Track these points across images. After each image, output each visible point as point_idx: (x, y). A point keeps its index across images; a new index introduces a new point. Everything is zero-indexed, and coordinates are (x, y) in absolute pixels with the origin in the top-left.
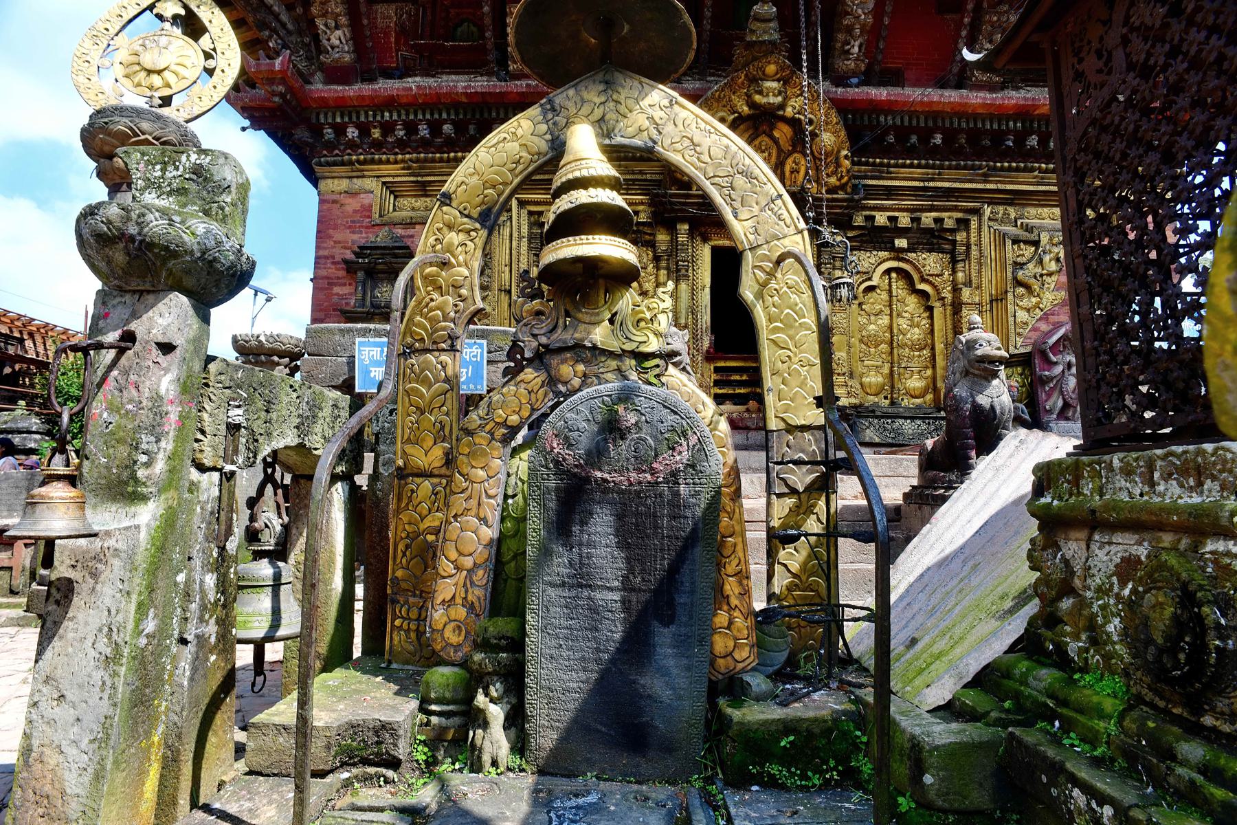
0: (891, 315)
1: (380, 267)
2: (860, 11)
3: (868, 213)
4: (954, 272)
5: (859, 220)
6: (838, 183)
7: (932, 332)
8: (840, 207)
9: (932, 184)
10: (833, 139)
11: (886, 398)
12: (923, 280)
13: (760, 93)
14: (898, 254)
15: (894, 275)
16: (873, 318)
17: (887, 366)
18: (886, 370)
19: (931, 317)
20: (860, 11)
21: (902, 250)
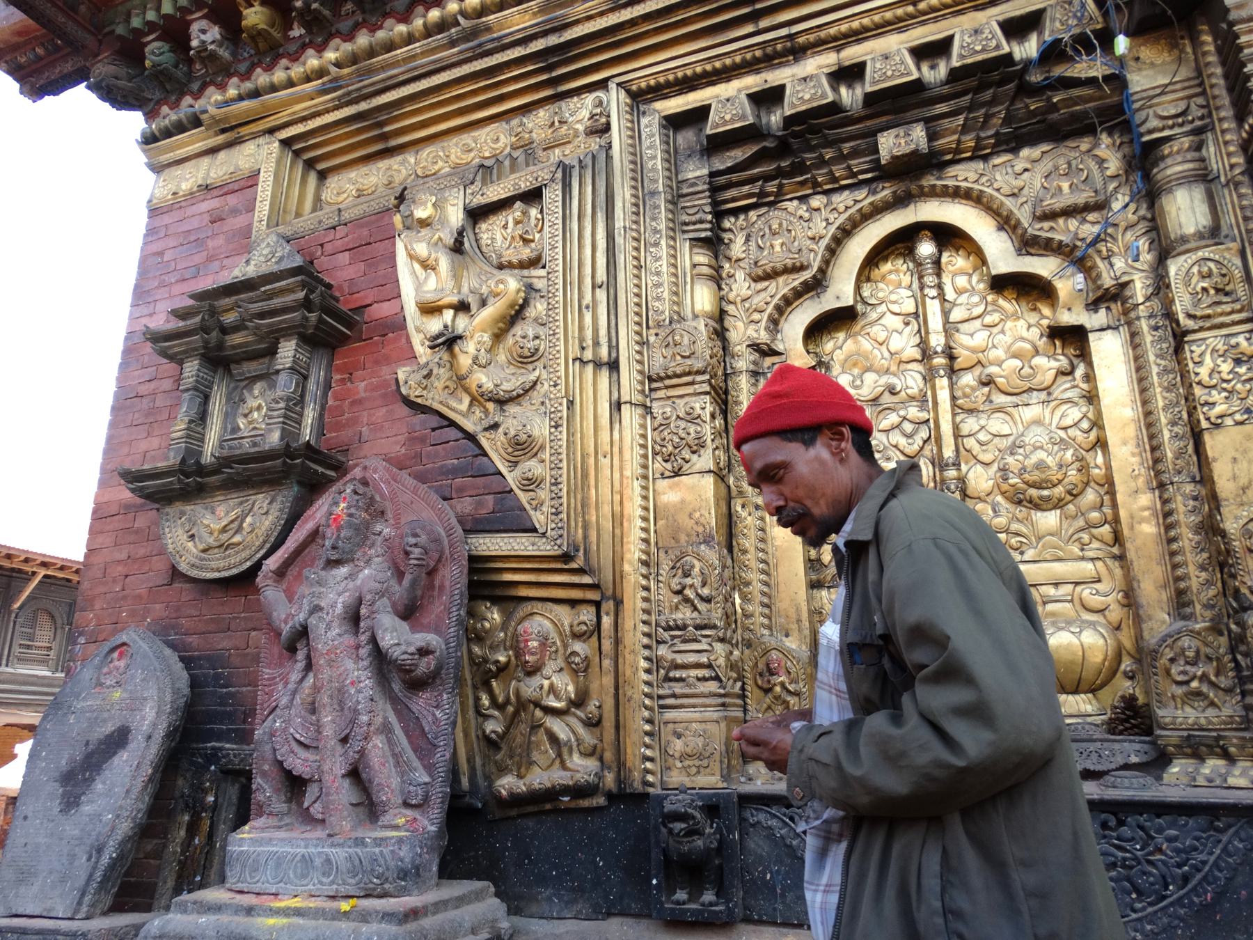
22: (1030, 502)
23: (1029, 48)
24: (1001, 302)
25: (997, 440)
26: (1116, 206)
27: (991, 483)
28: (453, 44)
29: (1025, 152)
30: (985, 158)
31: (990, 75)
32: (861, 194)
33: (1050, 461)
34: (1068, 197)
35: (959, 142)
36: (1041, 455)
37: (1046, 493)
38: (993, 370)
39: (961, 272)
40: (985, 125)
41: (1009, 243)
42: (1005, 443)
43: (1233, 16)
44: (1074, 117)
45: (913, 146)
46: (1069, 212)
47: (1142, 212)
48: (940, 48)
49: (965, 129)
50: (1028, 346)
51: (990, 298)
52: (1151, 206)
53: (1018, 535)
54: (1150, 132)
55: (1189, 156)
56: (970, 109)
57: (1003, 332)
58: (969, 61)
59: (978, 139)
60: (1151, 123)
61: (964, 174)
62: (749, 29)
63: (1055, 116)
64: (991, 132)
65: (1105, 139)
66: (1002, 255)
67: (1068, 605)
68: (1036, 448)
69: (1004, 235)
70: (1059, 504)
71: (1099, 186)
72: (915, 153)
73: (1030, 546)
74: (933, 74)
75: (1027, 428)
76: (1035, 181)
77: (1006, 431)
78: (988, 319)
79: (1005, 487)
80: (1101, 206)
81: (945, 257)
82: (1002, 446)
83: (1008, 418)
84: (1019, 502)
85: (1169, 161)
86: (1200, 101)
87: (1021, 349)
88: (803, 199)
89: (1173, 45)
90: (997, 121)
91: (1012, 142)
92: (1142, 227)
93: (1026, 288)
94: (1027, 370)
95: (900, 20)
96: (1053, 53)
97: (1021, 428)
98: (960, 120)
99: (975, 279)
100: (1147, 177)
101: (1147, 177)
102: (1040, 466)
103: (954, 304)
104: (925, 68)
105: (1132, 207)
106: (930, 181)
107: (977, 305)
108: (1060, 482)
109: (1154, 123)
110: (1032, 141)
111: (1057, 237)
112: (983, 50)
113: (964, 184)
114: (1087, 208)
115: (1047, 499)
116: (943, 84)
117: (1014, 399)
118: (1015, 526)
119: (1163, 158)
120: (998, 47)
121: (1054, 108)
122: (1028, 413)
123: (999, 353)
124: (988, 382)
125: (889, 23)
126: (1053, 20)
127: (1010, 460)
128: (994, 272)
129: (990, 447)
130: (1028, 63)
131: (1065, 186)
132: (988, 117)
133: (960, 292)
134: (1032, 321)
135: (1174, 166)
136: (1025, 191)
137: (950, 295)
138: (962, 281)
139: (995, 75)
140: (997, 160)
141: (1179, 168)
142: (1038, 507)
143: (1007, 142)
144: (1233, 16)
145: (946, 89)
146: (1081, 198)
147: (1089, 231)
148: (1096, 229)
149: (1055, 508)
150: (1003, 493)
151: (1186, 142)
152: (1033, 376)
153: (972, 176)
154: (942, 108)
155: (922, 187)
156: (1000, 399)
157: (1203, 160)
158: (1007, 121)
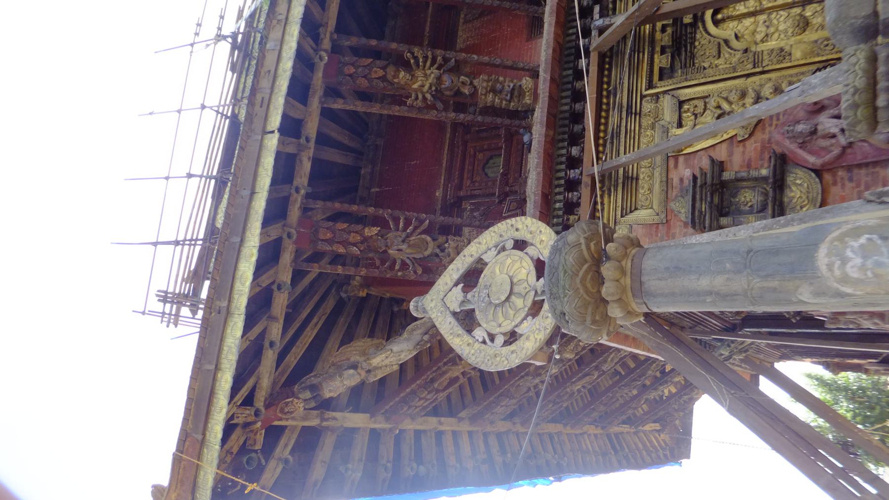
1: (716, 200)
28: (612, 143)
32: (698, 31)
62: (641, 55)
88: (695, 47)
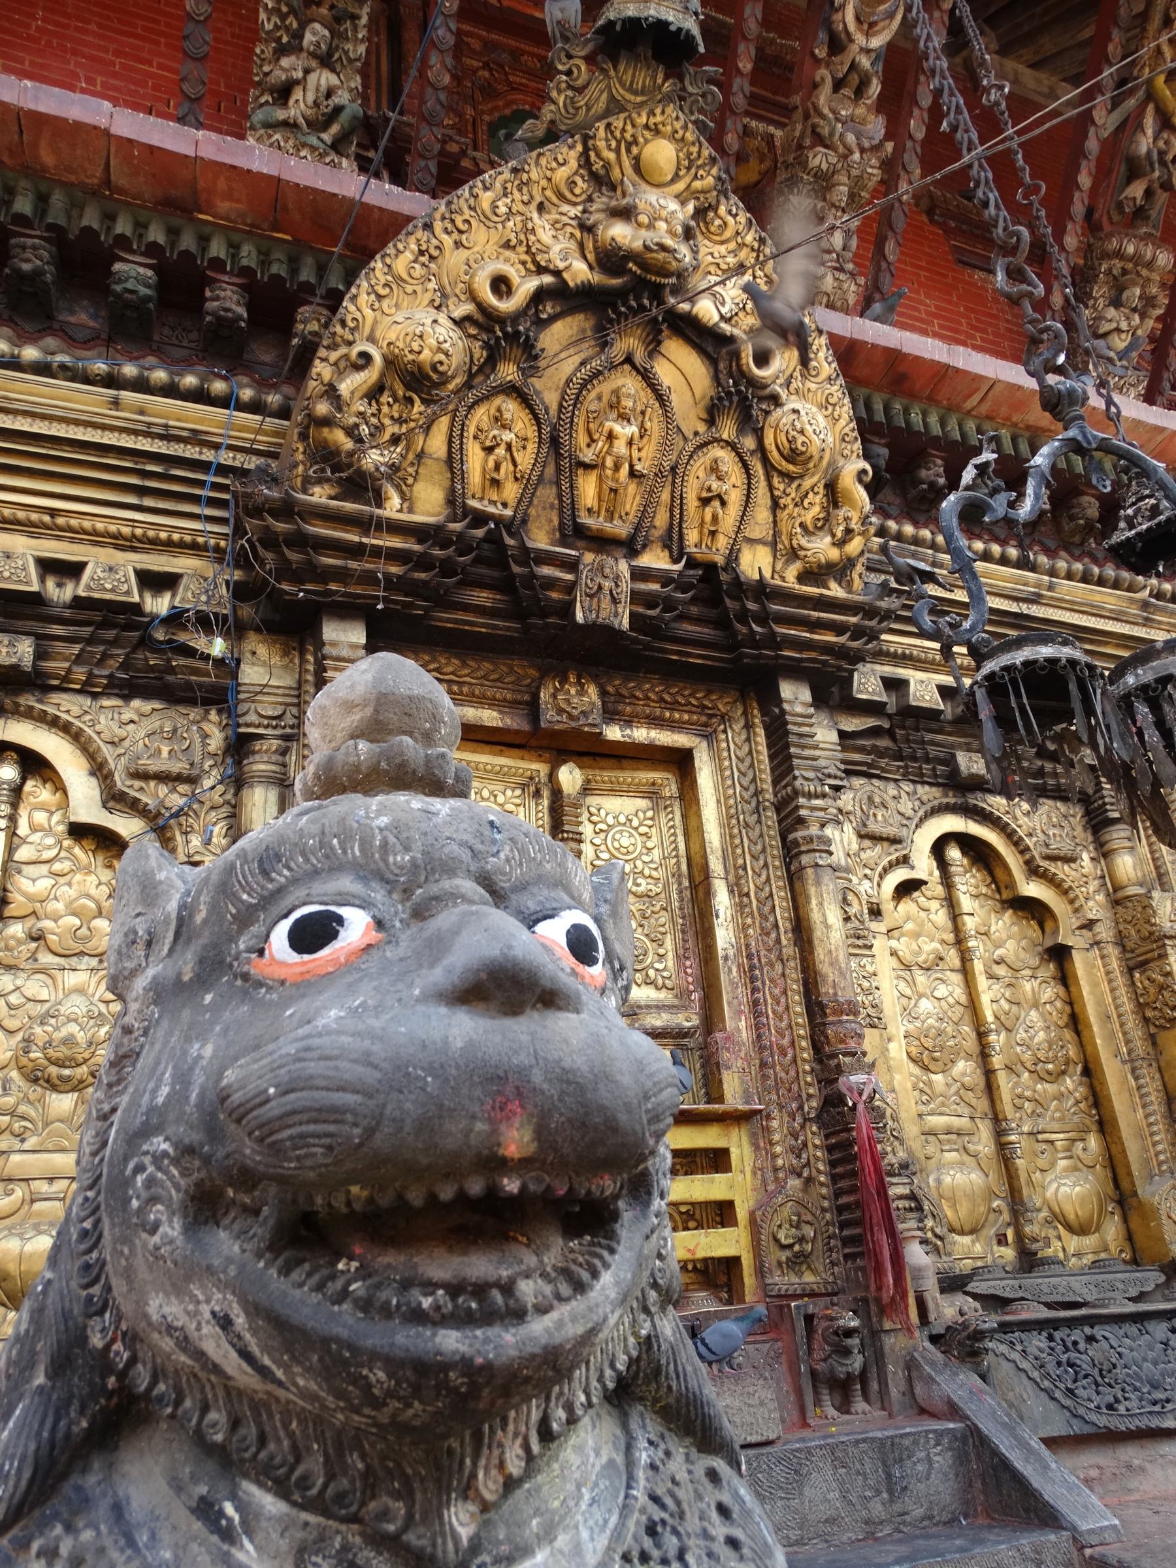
0: (966, 970)
2: (851, 138)
3: (888, 670)
4: (1104, 853)
5: (867, 683)
6: (834, 554)
7: (1075, 1021)
8: (839, 629)
9: (1036, 611)
10: (822, 422)
11: (1002, 1240)
12: (1033, 871)
13: (626, 214)
14: (961, 792)
15: (954, 853)
16: (921, 978)
17: (985, 1131)
18: (984, 1143)
19: (1065, 978)
20: (851, 138)
21: (977, 785)
22: (48, 1081)
23: (159, 605)
24: (77, 850)
25: (30, 1005)
26: (207, 783)
27: (9, 1054)
29: (136, 703)
30: (95, 696)
31: (108, 618)
33: (81, 1037)
34: (163, 763)
35: (69, 671)
36: (73, 1028)
37: (67, 1072)
38: (47, 924)
39: (42, 807)
40: (101, 663)
41: (97, 792)
42: (40, 1009)
43: (327, 650)
44: (189, 686)
45: (14, 660)
46: (162, 777)
47: (229, 796)
48: (73, 570)
49: (78, 660)
50: (93, 905)
51: (66, 843)
52: (236, 794)
53: (24, 1118)
54: (248, 725)
55: (274, 758)
56: (90, 641)
57: (69, 884)
58: (96, 595)
59: (90, 675)
60: (252, 718)
61: (67, 705)
63: (171, 678)
64: (106, 672)
65: (213, 715)
66: (85, 801)
67: (57, 1204)
68: (69, 1020)
69: (94, 782)
70: (78, 1086)
71: (197, 759)
72: (15, 668)
73: (34, 1133)
74: (60, 593)
75: (66, 996)
76: (138, 733)
77: (44, 995)
78: (57, 867)
79: (24, 1061)
80: (192, 780)
81: (29, 785)
82: (33, 1013)
83: (49, 981)
84: (35, 1081)
85: (257, 757)
86: (295, 711)
87: (84, 906)
89: (285, 653)
90: (113, 663)
91: (128, 690)
92: (225, 811)
93: (105, 842)
94: (84, 931)
95: (32, 524)
96: (175, 619)
97: (61, 995)
98: (76, 649)
99: (56, 817)
100: (238, 763)
101: (238, 763)
102: (69, 1041)
103: (24, 841)
104: (50, 583)
105: (220, 788)
106: (28, 700)
107: (49, 848)
108: (86, 1061)
109: (252, 718)
110: (146, 693)
111: (145, 799)
112: (113, 590)
113: (64, 716)
114: (179, 778)
115: (69, 1079)
116: (65, 606)
117: (61, 961)
118: (23, 1109)
119: (254, 753)
120: (128, 593)
121: (172, 670)
122: (72, 979)
123: (60, 906)
124: (38, 937)
125: (19, 523)
126: (187, 589)
127: (38, 1030)
128: (73, 819)
129: (20, 1012)
130: (154, 617)
131: (165, 750)
132: (105, 657)
133: (34, 829)
134: (104, 879)
135: (260, 765)
136: (126, 743)
137: (23, 829)
138: (40, 817)
139: (121, 618)
140: (106, 702)
141: (263, 767)
142: (54, 1088)
143: (120, 687)
144: (327, 650)
145: (67, 613)
146: (177, 767)
147: (176, 801)
148: (182, 801)
149: (73, 1090)
150: (20, 1068)
151: (275, 744)
152: (89, 939)
153: (76, 710)
154: (58, 630)
155: (17, 705)
156: (46, 959)
157: (284, 765)
158: (124, 666)
